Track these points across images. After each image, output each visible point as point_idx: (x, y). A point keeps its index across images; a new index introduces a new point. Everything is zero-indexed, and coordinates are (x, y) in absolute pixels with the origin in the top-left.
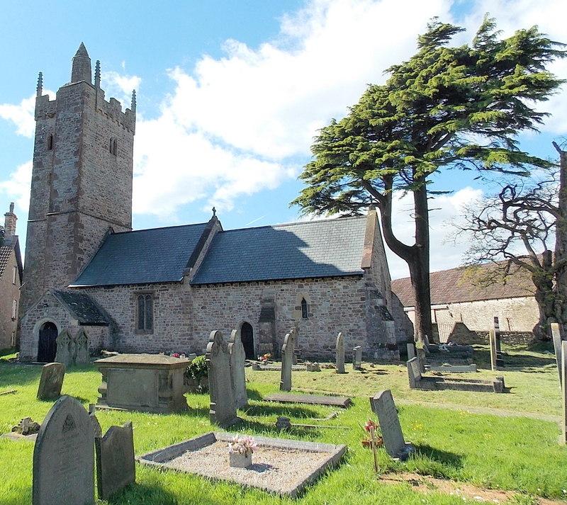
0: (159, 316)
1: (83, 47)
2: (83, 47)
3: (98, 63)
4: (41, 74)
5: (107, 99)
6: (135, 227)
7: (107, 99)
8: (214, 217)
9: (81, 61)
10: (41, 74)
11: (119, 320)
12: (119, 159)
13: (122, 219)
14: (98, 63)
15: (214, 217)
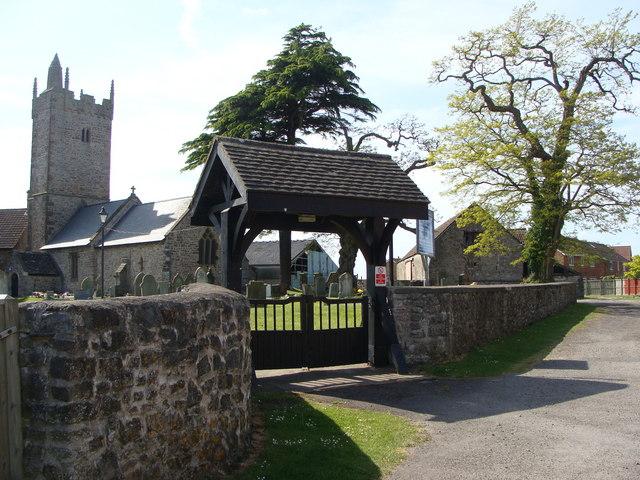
0: (81, 269)
1: (56, 57)
2: (56, 57)
3: (67, 69)
4: (36, 79)
5: (77, 97)
6: (113, 198)
7: (77, 97)
8: (133, 195)
9: (55, 70)
10: (36, 79)
11: (64, 272)
12: (92, 144)
13: (97, 193)
14: (67, 69)
15: (133, 195)
